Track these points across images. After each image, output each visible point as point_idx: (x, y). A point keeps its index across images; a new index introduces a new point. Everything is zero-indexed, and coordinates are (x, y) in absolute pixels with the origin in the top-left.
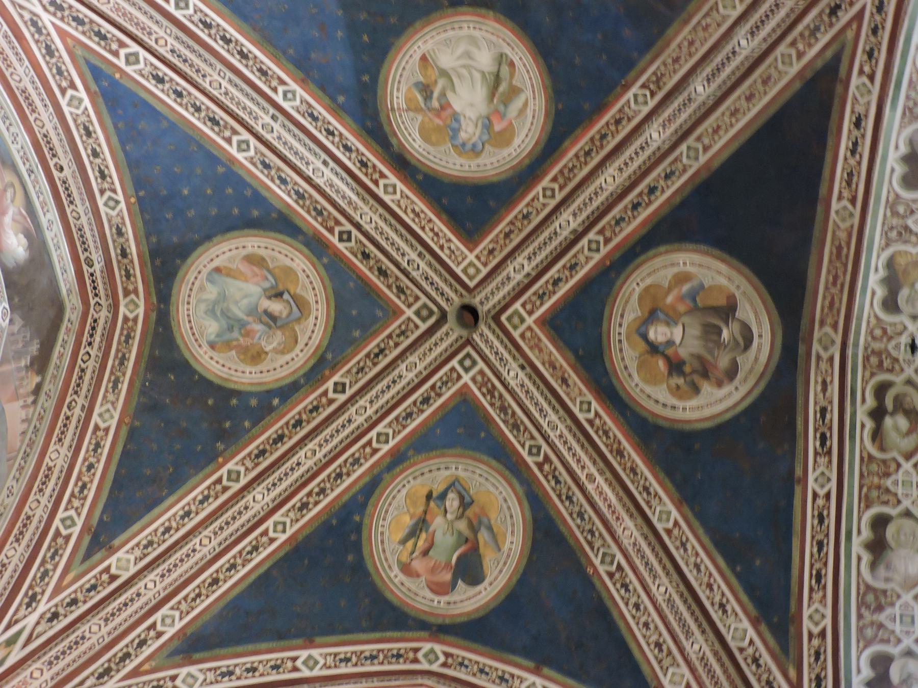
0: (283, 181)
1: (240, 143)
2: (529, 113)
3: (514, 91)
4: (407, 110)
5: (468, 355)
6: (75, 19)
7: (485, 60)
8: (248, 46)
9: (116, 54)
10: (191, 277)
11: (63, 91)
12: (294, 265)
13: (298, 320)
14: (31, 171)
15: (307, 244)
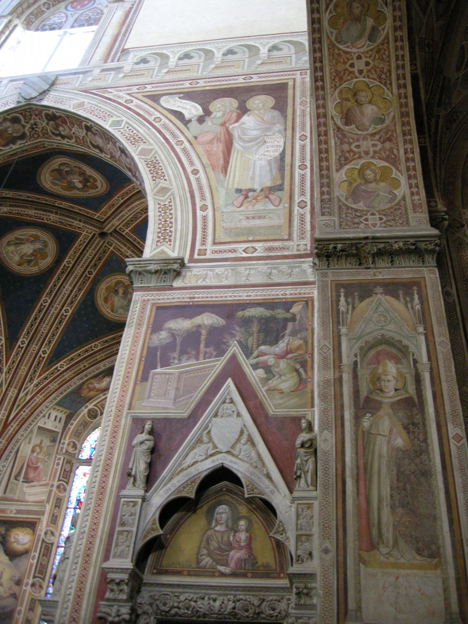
0: (76, 296)
1: (66, 312)
2: (22, 233)
3: (17, 239)
4: (38, 265)
5: (120, 229)
6: (34, 373)
7: (11, 248)
8: (32, 318)
9: (44, 358)
10: (116, 318)
11: (59, 370)
12: (104, 288)
13: (123, 284)
14: (86, 376)
15: (96, 285)
